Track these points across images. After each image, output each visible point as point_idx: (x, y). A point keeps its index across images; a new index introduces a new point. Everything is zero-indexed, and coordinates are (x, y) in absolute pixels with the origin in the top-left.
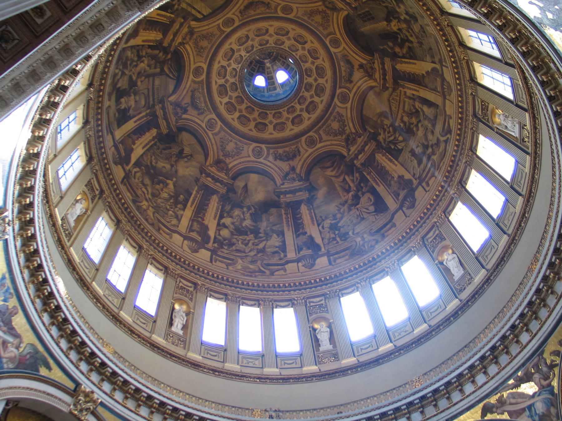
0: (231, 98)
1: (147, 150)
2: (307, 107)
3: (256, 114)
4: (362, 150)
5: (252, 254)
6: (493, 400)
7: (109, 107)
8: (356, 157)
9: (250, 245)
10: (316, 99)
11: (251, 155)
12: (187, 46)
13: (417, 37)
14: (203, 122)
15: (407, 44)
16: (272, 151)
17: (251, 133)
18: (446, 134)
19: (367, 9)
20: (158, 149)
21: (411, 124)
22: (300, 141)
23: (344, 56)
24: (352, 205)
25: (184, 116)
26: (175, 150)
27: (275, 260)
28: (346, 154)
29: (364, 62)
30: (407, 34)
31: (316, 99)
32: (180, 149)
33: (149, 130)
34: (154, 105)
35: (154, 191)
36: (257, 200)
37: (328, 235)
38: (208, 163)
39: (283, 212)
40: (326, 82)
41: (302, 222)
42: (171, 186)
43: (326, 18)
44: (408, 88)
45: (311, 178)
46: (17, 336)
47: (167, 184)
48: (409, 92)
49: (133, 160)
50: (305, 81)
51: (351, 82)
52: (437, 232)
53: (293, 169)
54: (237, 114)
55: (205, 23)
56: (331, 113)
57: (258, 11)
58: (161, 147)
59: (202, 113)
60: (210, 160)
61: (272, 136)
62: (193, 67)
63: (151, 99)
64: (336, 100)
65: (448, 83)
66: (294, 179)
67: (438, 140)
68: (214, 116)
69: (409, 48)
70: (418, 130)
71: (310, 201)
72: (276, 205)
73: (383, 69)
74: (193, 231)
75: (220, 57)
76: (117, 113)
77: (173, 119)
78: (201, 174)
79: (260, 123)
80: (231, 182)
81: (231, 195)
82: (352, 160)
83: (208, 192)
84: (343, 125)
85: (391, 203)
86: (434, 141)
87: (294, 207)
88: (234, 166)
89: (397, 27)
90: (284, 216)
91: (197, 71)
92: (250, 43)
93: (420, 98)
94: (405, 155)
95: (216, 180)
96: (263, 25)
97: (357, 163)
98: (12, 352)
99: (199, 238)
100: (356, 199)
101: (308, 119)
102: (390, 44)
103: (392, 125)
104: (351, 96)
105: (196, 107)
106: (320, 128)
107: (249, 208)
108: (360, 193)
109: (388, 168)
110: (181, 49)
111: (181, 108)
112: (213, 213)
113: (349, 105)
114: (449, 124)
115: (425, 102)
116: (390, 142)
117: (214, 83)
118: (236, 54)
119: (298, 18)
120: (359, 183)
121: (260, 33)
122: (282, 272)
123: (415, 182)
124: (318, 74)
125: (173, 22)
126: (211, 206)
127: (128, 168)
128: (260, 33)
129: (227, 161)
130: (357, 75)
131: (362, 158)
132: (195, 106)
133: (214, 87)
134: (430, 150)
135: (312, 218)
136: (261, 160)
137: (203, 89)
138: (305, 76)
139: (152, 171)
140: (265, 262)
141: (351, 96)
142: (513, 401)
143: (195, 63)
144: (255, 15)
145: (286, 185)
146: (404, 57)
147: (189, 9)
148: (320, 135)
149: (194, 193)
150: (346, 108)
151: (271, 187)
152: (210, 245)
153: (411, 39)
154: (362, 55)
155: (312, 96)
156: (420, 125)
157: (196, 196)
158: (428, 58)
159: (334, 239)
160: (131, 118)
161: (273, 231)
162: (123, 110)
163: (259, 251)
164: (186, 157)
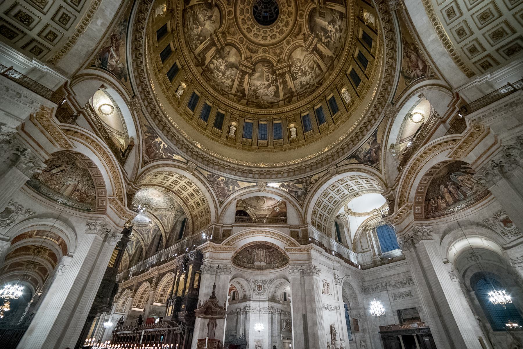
1: (198, 4)
2: (272, 36)
3: (250, 23)
4: (282, 68)
5: (219, 82)
6: (286, 184)
8: (278, 69)
9: (219, 77)
10: (278, 35)
11: (238, 39)
14: (227, 9)
15: (329, 39)
16: (247, 44)
17: (243, 30)
18: (319, 84)
19: (325, 12)
20: (203, 7)
21: (307, 71)
22: (261, 48)
23: (301, 25)
24: (265, 87)
26: (209, 14)
27: (226, 90)
28: (275, 66)
29: (307, 33)
30: (332, 35)
31: (278, 35)
32: (211, 15)
35: (192, 27)
36: (231, 60)
37: (251, 93)
38: (219, 30)
39: (238, 72)
40: (286, 30)
41: (243, 82)
42: (200, 30)
44: (316, 57)
45: (256, 66)
47: (198, 28)
49: (190, 5)
50: (278, 24)
51: (296, 38)
52: (293, 117)
53: (251, 57)
56: (279, 45)
58: (205, 7)
59: (229, 5)
60: (221, 30)
64: (285, 41)
65: (334, 66)
66: (249, 62)
67: (314, 84)
68: (233, 10)
69: (329, 41)
70: (308, 75)
71: (251, 75)
72: (237, 68)
73: (312, 42)
74: (200, 57)
79: (249, 28)
80: (224, 45)
81: (221, 51)
82: (276, 70)
83: (213, 44)
84: (281, 53)
85: (281, 95)
86: (312, 84)
87: (244, 73)
88: (229, 40)
89: (330, 29)
90: (238, 74)
93: (318, 63)
94: (297, 82)
95: (219, 40)
97: (277, 72)
99: (201, 62)
100: (269, 85)
101: (269, 41)
102: (322, 34)
103: (300, 67)
104: (292, 44)
106: (272, 48)
107: (226, 62)
108: (272, 84)
109: (288, 82)
112: (211, 55)
113: (289, 47)
114: (322, 81)
115: (319, 66)
116: (295, 73)
120: (274, 81)
122: (227, 96)
123: (295, 94)
124: (285, 24)
126: (211, 50)
129: (228, 35)
130: (301, 36)
131: (280, 71)
134: (308, 86)
135: (248, 82)
136: (241, 45)
138: (280, 22)
139: (195, 17)
140: (222, 88)
141: (292, 44)
142: (292, 187)
145: (245, 62)
146: (323, 43)
148: (269, 51)
149: (207, 40)
150: (287, 47)
151: (238, 59)
152: (204, 67)
154: (308, 30)
155: (277, 32)
156: (311, 74)
157: (207, 42)
158: (333, 51)
159: (253, 96)
161: (231, 78)
163: (222, 82)
164: (212, 21)
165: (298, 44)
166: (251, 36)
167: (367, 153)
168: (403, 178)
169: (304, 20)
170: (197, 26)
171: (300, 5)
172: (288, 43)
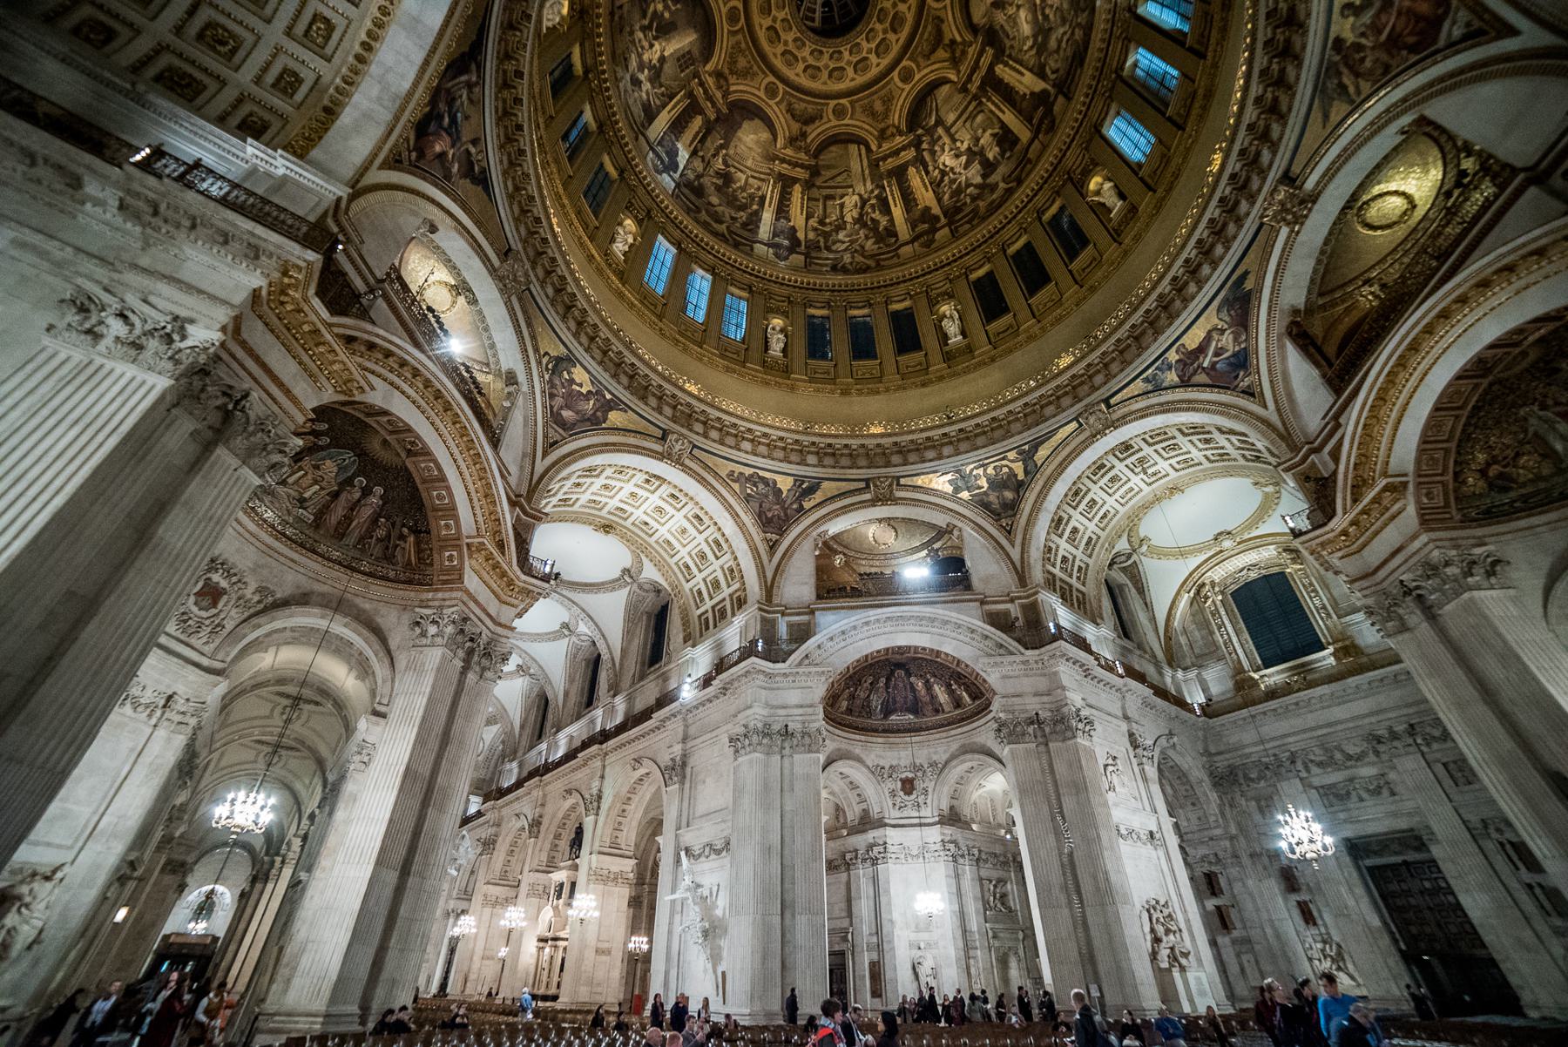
7: (1004, 180)
13: (633, 42)
25: (959, 39)
33: (1001, 81)
34: (975, 97)
43: (732, 62)
46: (1208, 338)
55: (863, 134)
58: (1008, 43)
62: (907, 87)
63: (971, 108)
69: (644, 17)
75: (874, 72)
77: (972, 51)
91: (907, 77)
98: (1227, 340)
102: (667, 15)
105: (939, 34)
110: (903, 127)
111: (953, 52)
125: (890, 173)
144: (809, 102)
153: (640, 35)
160: (1003, 125)
167: (453, 120)
168: (428, 369)
170: (1043, 14)
171: (743, 45)
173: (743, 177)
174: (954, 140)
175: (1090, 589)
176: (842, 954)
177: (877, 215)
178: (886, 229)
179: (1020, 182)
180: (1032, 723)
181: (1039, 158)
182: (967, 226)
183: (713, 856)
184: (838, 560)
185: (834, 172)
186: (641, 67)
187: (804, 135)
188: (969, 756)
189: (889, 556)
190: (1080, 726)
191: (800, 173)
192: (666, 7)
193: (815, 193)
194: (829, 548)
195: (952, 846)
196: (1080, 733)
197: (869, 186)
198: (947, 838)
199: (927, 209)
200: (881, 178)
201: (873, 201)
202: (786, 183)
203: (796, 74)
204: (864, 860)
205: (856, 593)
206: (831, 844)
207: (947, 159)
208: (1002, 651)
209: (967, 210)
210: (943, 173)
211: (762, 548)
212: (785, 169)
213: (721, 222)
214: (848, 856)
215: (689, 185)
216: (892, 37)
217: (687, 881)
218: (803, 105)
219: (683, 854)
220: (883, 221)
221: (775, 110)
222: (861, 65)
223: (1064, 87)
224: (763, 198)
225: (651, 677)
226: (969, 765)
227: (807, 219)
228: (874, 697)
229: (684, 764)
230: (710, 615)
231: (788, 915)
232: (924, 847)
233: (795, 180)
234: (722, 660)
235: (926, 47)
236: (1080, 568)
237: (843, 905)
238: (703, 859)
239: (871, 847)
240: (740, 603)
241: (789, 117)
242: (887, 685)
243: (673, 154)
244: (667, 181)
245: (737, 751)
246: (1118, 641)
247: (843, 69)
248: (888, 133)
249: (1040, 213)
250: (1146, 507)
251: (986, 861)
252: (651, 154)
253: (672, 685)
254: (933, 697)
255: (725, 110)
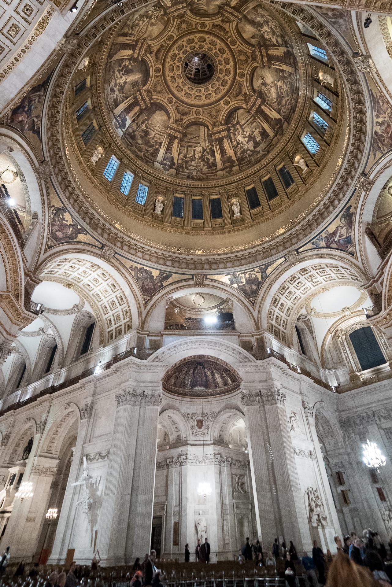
0: (224, 76)
3: (219, 58)
10: (185, 44)
12: (221, 120)
17: (229, 53)
23: (157, 61)
25: (248, 93)
29: (148, 55)
31: (185, 44)
33: (263, 112)
34: (253, 116)
38: (258, 65)
40: (174, 50)
43: (155, 87)
48: (132, 38)
54: (227, 67)
55: (207, 123)
57: (183, 108)
58: (267, 99)
59: (241, 84)
60: (256, 64)
61: (221, 43)
62: (226, 107)
63: (251, 120)
64: (175, 39)
68: (237, 77)
73: (140, 50)
75: (213, 99)
76: (264, 140)
77: (253, 99)
78: (265, 66)
83: (271, 58)
91: (226, 103)
92: (196, 94)
96: (185, 99)
101: (196, 37)
102: (130, 67)
105: (240, 91)
110: (223, 122)
111: (246, 97)
117: (225, 90)
118: (206, 94)
119: (168, 93)
121: (188, 95)
124: (176, 57)
125: (216, 140)
127: (283, 119)
128: (188, 95)
129: (249, 54)
130: (155, 49)
132: (240, 92)
133: (227, 88)
137: (231, 93)
143: (224, 108)
144: (185, 107)
146: (126, 59)
147: (207, 138)
153: (117, 73)
154: (147, 59)
155: (186, 47)
160: (263, 129)
162: (262, 137)
165: (157, 40)
166: (220, 44)
169: (154, 68)
171: (160, 81)
172: (170, 38)
173: (154, 133)
174: (244, 131)
175: (288, 331)
176: (160, 517)
177: (209, 157)
178: (212, 163)
179: (268, 152)
180: (258, 396)
181: (276, 145)
182: (246, 167)
183: (100, 460)
184: (176, 310)
185: (193, 136)
186: (116, 85)
187: (182, 119)
188: (229, 410)
189: (199, 310)
190: (279, 398)
191: (179, 135)
192: (130, 64)
193: (184, 144)
194: (173, 304)
195: (218, 457)
196: (279, 401)
197: (207, 144)
198: (217, 452)
199: (230, 157)
200: (212, 141)
201: (208, 151)
202: (172, 138)
203: (181, 95)
204: (176, 463)
205: (182, 328)
206: (161, 453)
207: (240, 138)
208: (246, 360)
209: (246, 160)
210: (238, 144)
211: (142, 303)
212: (172, 132)
213: (141, 151)
214: (168, 460)
215: (129, 134)
216: (221, 87)
217: (85, 475)
218: (183, 108)
219: (85, 458)
220: (211, 159)
221: (171, 108)
222: (208, 96)
223: (288, 119)
224: (161, 143)
225: (81, 360)
226: (229, 414)
227: (179, 154)
228: (187, 378)
229: (92, 408)
230: (114, 332)
231: (134, 495)
232: (205, 457)
233: (175, 138)
234: (117, 356)
235: (235, 94)
236: (284, 321)
237: (163, 488)
238: (95, 461)
239: (179, 456)
240: (129, 327)
241: (176, 111)
242: (194, 372)
243: (124, 121)
244: (120, 132)
245: (119, 403)
246: (299, 356)
247: (200, 96)
248: (217, 124)
249: (276, 167)
250: (313, 296)
251: (235, 465)
252: (114, 120)
253: (91, 366)
254: (215, 380)
255: (149, 105)
